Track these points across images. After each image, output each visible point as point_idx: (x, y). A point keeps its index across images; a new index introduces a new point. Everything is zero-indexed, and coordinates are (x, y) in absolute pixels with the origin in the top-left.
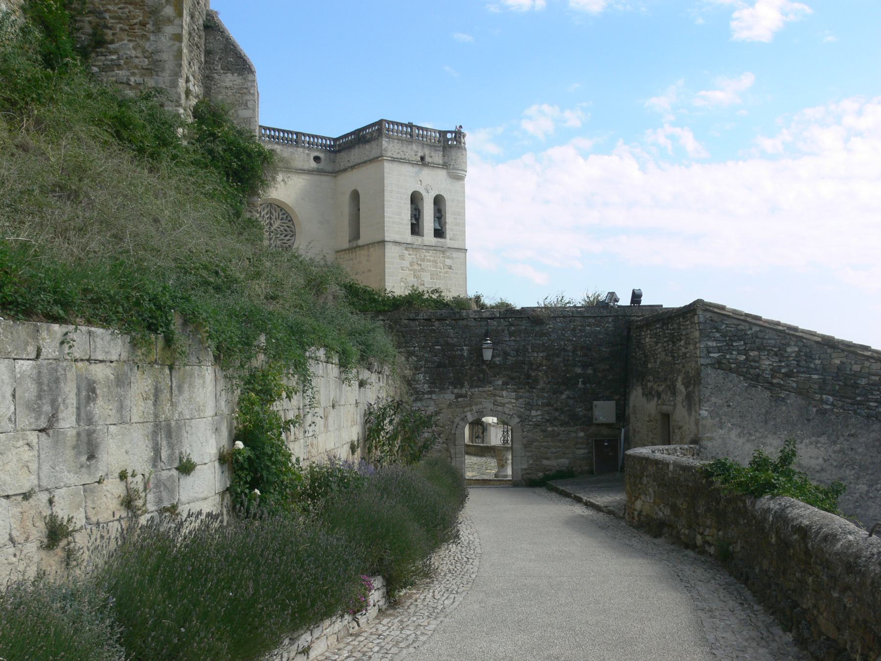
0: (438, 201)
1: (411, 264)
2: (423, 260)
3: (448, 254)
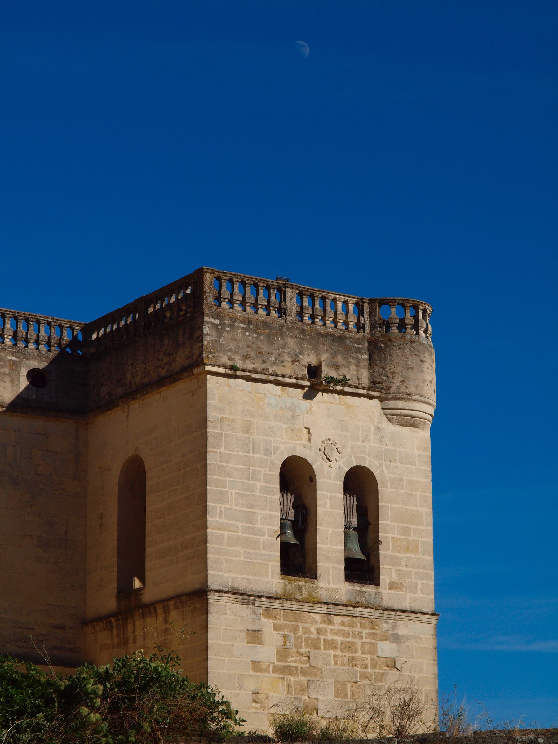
0: (359, 484)
1: (283, 653)
3: (385, 626)
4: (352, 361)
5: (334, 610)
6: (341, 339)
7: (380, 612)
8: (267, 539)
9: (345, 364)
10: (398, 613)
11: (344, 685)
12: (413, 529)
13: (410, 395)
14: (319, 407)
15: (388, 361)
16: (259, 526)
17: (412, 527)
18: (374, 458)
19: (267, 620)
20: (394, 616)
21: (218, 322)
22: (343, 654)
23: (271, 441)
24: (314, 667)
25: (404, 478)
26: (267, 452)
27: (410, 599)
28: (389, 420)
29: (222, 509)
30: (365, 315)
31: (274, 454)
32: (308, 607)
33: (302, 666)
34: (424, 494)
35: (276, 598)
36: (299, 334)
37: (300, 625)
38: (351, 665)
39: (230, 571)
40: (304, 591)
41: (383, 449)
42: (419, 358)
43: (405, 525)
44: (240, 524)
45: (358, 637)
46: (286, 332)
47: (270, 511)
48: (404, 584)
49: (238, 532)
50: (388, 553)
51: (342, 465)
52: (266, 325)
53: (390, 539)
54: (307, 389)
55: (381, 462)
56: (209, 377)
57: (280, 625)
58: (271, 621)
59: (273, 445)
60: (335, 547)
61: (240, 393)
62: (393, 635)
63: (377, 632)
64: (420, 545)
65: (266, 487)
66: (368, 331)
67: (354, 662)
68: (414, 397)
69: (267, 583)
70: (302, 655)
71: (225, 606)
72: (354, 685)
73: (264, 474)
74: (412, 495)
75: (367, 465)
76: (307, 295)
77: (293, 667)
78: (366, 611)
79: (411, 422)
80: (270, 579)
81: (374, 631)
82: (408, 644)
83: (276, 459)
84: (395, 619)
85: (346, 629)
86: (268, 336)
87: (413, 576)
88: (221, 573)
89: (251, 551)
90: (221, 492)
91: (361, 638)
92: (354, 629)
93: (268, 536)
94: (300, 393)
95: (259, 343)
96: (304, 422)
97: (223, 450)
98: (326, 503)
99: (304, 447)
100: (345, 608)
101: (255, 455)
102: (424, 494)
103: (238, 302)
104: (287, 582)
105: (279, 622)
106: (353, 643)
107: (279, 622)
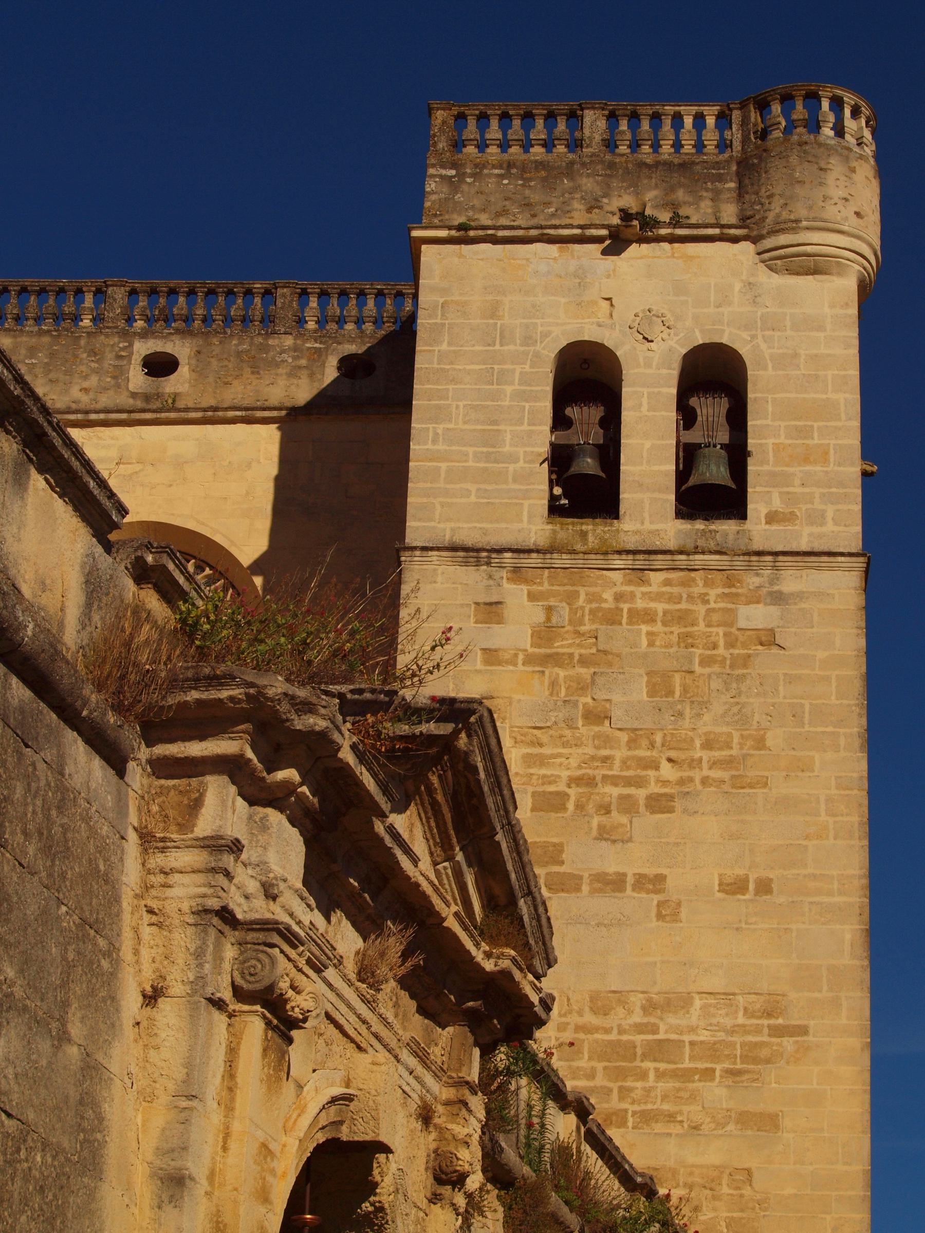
1: (545, 633)
2: (612, 618)
3: (753, 581)
4: (705, 194)
5: (647, 563)
6: (685, 166)
7: (741, 558)
8: (522, 468)
9: (691, 200)
10: (781, 558)
11: (666, 676)
12: (819, 428)
13: (797, 221)
14: (632, 266)
15: (762, 181)
16: (507, 449)
17: (816, 425)
18: (739, 328)
19: (515, 586)
20: (771, 564)
21: (453, 172)
22: (667, 629)
23: (536, 323)
24: (605, 652)
25: (802, 352)
26: (528, 340)
27: (810, 535)
28: (771, 269)
29: (440, 431)
30: (734, 127)
31: (541, 342)
32: (596, 561)
33: (583, 651)
34: (843, 373)
35: (530, 551)
36: (603, 169)
37: (582, 592)
38: (682, 645)
39: (449, 520)
40: (591, 538)
41: (759, 314)
42: (816, 166)
43: (801, 423)
44: (470, 450)
45: (699, 601)
46: (578, 171)
47: (529, 425)
48: (798, 514)
49: (466, 461)
50: (766, 468)
51: (674, 345)
52: (540, 165)
53: (771, 447)
54: (608, 242)
55: (754, 332)
56: (424, 247)
57: (541, 592)
58: (525, 588)
59: (540, 329)
60: (656, 468)
61: (481, 263)
62: (770, 594)
63: (740, 591)
64: (832, 452)
65: (524, 392)
66: (740, 148)
67: (690, 641)
68: (804, 223)
69: (519, 531)
70: (583, 635)
71: (435, 570)
72: (688, 676)
73: (521, 373)
74: (817, 377)
75: (725, 340)
76: (625, 116)
77: (563, 654)
78: (713, 560)
79: (813, 266)
80: (525, 525)
81: (733, 590)
82: (803, 605)
83: (544, 349)
84: (775, 568)
85: (675, 590)
86: (544, 180)
87: (817, 500)
88: (432, 524)
89: (489, 487)
90: (438, 407)
91: (708, 602)
92: (691, 590)
93: (525, 462)
94: (595, 249)
95: (527, 192)
96: (600, 290)
97: (444, 347)
98: (641, 405)
99: (600, 326)
100: (669, 557)
101: (506, 348)
102: (843, 373)
103: (494, 142)
104: (558, 528)
105: (540, 588)
106: (688, 612)
107: (540, 588)
